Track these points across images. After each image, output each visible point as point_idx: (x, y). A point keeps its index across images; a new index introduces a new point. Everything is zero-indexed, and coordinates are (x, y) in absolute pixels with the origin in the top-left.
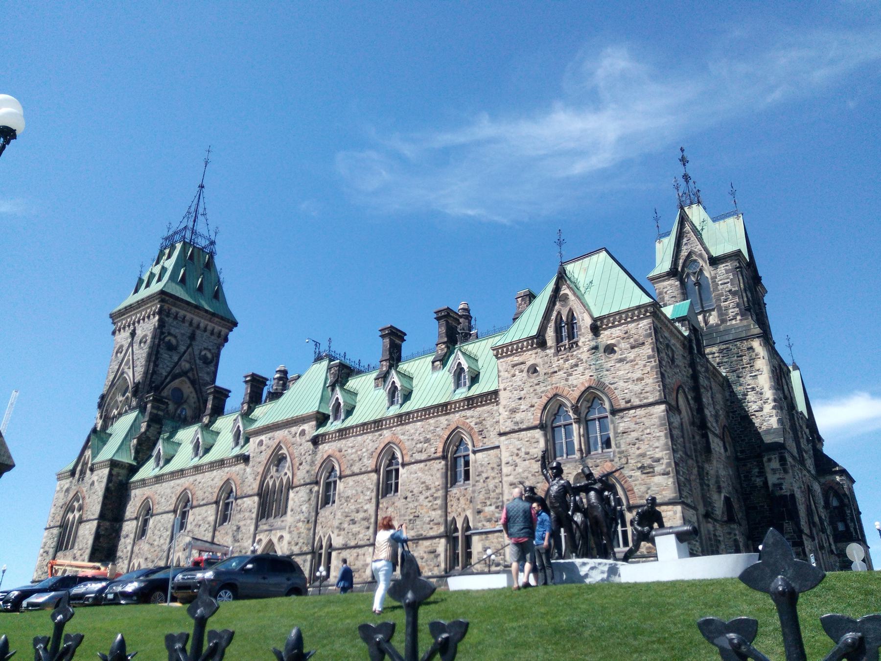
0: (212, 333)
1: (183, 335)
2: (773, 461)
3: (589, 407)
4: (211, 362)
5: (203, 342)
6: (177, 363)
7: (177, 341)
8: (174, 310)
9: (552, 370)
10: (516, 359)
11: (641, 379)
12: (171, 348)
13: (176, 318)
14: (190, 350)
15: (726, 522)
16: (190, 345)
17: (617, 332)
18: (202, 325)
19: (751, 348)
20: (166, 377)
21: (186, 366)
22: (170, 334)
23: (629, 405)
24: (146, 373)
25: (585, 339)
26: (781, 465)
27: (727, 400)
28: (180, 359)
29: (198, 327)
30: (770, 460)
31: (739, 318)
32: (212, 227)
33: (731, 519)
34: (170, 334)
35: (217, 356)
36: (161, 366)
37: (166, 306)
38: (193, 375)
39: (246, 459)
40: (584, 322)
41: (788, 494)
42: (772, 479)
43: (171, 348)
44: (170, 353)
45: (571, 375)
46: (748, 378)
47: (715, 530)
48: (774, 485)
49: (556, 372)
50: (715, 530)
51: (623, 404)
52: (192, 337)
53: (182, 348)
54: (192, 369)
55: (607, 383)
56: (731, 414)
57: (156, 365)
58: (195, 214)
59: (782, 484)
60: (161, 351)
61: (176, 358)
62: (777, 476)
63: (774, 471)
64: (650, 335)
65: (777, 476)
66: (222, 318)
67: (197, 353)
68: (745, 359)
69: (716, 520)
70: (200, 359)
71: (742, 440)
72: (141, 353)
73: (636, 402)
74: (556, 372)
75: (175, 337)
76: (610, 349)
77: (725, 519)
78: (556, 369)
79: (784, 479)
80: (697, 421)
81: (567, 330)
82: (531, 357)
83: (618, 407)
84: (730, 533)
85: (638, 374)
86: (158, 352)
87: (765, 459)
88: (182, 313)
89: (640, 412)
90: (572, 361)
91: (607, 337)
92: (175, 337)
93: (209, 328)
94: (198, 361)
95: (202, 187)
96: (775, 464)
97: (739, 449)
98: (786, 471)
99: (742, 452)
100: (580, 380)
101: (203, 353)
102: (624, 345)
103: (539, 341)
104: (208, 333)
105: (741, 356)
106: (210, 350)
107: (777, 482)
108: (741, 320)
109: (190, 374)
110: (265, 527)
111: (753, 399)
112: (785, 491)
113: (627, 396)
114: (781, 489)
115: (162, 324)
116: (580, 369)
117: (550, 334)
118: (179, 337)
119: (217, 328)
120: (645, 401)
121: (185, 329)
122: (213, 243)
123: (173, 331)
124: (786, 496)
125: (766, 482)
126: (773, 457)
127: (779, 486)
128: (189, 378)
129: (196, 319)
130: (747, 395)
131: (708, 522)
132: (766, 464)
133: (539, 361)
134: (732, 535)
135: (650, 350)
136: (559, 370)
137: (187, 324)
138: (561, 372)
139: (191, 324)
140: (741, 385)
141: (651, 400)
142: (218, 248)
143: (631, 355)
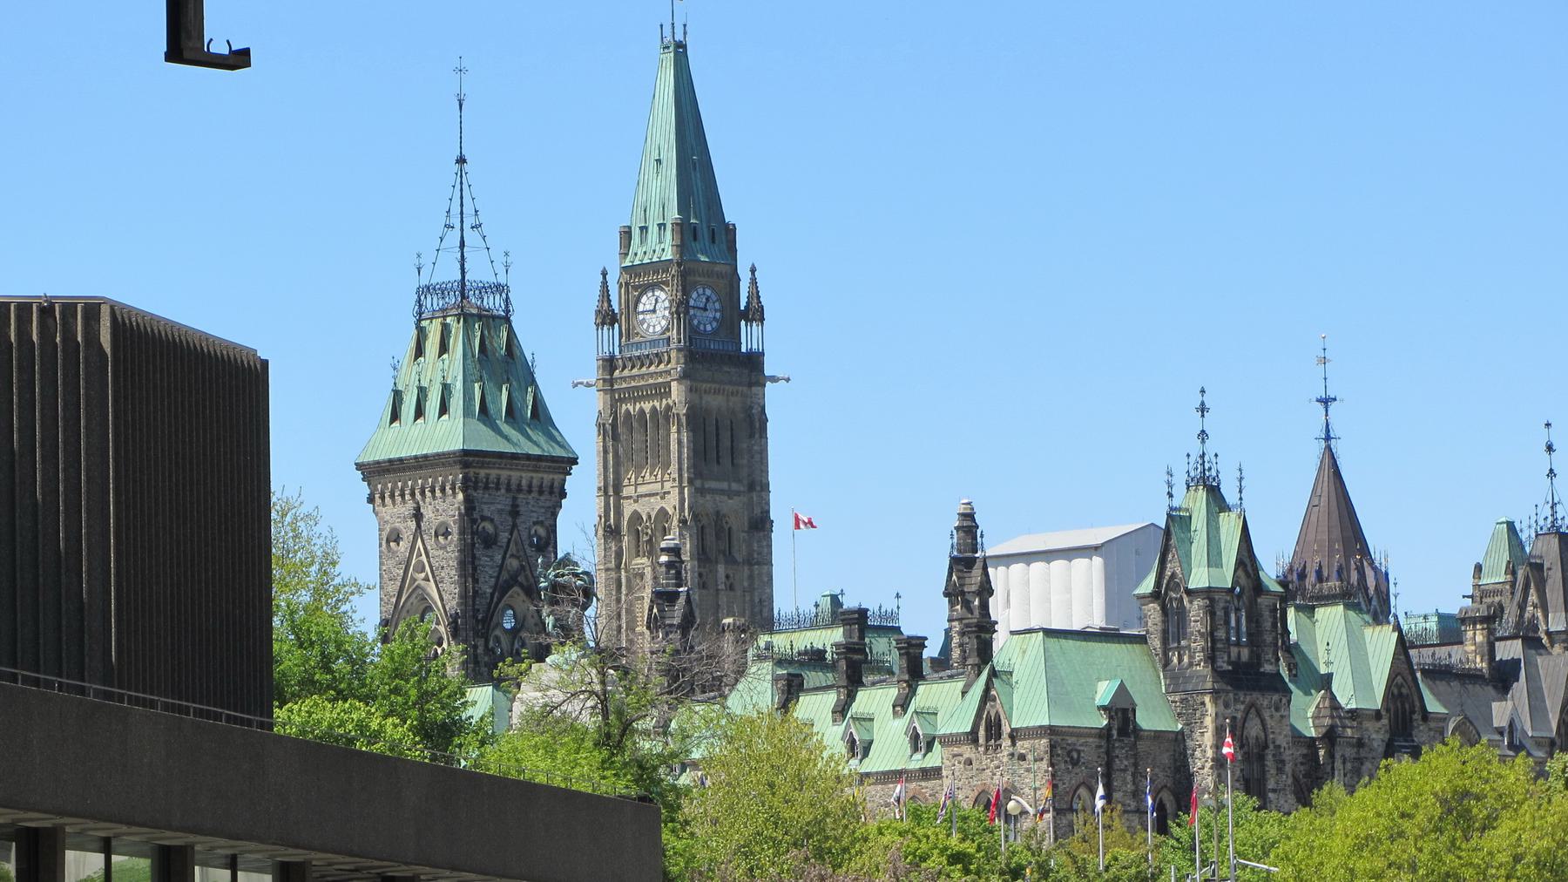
0: (541, 492)
1: (500, 512)
5: (531, 507)
7: (496, 528)
10: (956, 750)
12: (489, 542)
13: (486, 488)
16: (514, 526)
17: (1027, 744)
19: (1203, 703)
20: (492, 595)
22: (484, 518)
24: (464, 596)
25: (1006, 742)
28: (504, 558)
29: (519, 490)
34: (484, 518)
35: (552, 530)
36: (481, 580)
37: (471, 471)
40: (1006, 729)
43: (489, 542)
52: (515, 512)
53: (504, 536)
57: (476, 581)
60: (478, 553)
61: (498, 558)
67: (525, 535)
72: (446, 556)
75: (492, 520)
76: (1022, 757)
81: (994, 729)
82: (967, 751)
86: (474, 557)
88: (494, 473)
91: (1023, 746)
92: (492, 520)
93: (535, 482)
95: (461, 160)
103: (972, 738)
115: (468, 500)
117: (982, 732)
118: (496, 518)
119: (547, 477)
121: (502, 500)
123: (487, 513)
128: (521, 586)
133: (973, 756)
139: (508, 490)
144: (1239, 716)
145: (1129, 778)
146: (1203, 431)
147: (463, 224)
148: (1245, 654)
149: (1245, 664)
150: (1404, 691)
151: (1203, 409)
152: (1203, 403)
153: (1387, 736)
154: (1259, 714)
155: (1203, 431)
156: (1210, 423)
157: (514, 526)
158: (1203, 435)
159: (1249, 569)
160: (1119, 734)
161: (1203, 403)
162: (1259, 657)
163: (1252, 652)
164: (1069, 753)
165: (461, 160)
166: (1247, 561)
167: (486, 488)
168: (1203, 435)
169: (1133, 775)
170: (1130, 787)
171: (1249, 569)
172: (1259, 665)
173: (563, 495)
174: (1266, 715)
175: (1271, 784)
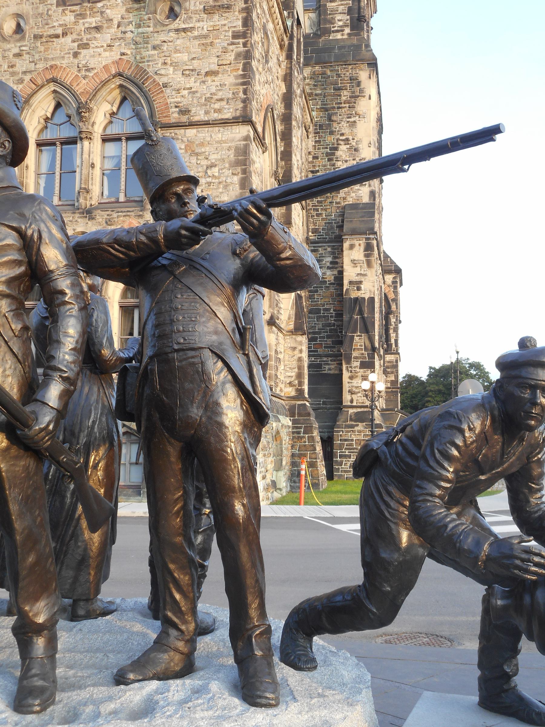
2: (357, 248)
3: (113, 114)
9: (52, 32)
15: (291, 331)
19: (355, 81)
23: (184, 119)
26: (366, 256)
27: (309, 153)
30: (352, 247)
31: (347, 30)
33: (298, 330)
41: (367, 297)
45: (86, 46)
47: (277, 344)
49: (57, 36)
50: (277, 344)
51: (174, 116)
55: (151, 71)
59: (361, 282)
62: (358, 270)
63: (354, 262)
65: (358, 270)
68: (345, 95)
69: (280, 329)
71: (318, 215)
73: (200, 115)
74: (57, 36)
77: (292, 327)
78: (59, 31)
79: (365, 275)
80: (281, 172)
83: (165, 120)
84: (294, 349)
87: (346, 245)
89: (204, 134)
90: (92, 21)
96: (358, 253)
97: (311, 227)
98: (369, 264)
99: (315, 231)
105: (340, 89)
107: (357, 279)
108: (349, 34)
111: (344, 157)
113: (184, 102)
114: (359, 289)
116: (105, 37)
120: (216, 116)
124: (364, 298)
125: (339, 278)
126: (357, 243)
127: (357, 285)
130: (336, 149)
131: (270, 332)
132: (345, 253)
134: (297, 352)
135: (240, 23)
136: (65, 34)
138: (69, 39)
140: (332, 133)
141: (228, 115)
143: (205, 25)
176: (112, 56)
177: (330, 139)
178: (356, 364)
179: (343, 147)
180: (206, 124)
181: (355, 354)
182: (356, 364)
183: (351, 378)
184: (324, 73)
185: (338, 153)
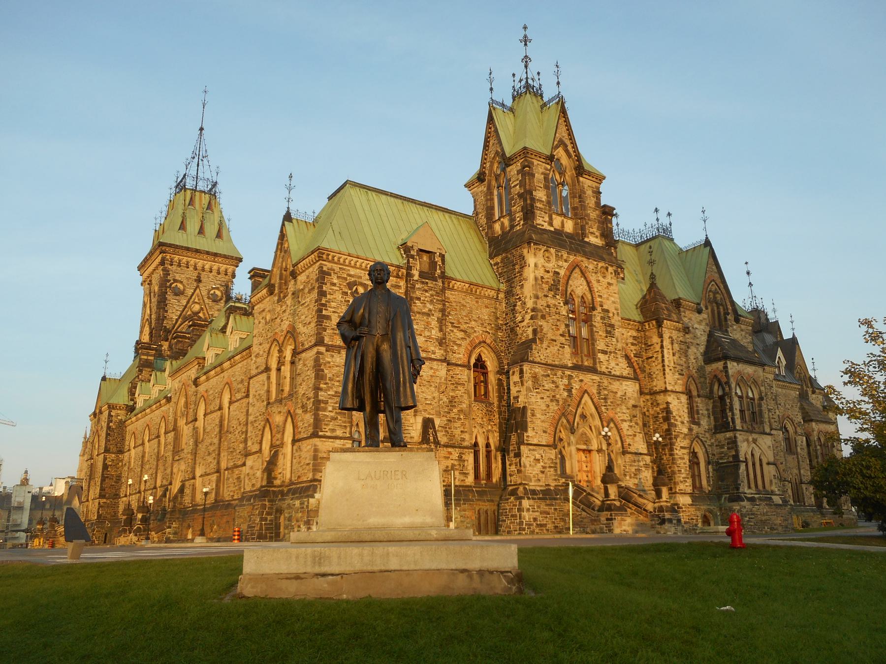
0: (219, 273)
4: (221, 299)
6: (186, 307)
8: (176, 258)
11: (310, 323)
13: (179, 265)
14: (198, 290)
16: (198, 287)
18: (207, 267)
20: (177, 320)
21: (196, 308)
28: (188, 302)
29: (203, 270)
30: (514, 373)
32: (213, 168)
34: (175, 281)
38: (204, 314)
39: (169, 400)
42: (514, 390)
44: (177, 297)
46: (518, 287)
48: (514, 398)
52: (199, 280)
53: (189, 292)
54: (202, 309)
56: (504, 327)
58: (199, 156)
61: (184, 302)
62: (517, 389)
63: (515, 383)
64: (317, 280)
66: (225, 257)
70: (209, 298)
85: (308, 320)
87: (511, 372)
92: (181, 282)
93: (215, 268)
94: (207, 301)
95: (201, 129)
98: (522, 385)
100: (285, 326)
101: (212, 292)
102: (306, 290)
104: (214, 273)
106: (217, 288)
107: (516, 394)
109: (201, 315)
110: (177, 458)
112: (521, 404)
118: (185, 281)
119: (223, 267)
121: (192, 274)
122: (215, 185)
127: (517, 398)
129: (200, 263)
130: (515, 306)
137: (191, 268)
139: (195, 269)
142: (219, 188)
144: (562, 272)
145: (434, 323)
146: (526, 57)
147: (199, 156)
148: (569, 227)
149: (569, 236)
150: (719, 297)
151: (526, 41)
152: (525, 36)
153: (708, 329)
154: (583, 274)
155: (526, 57)
156: (531, 50)
157: (198, 287)
158: (526, 60)
159: (570, 147)
160: (422, 275)
161: (525, 36)
162: (583, 228)
163: (576, 224)
164: (350, 285)
165: (201, 129)
166: (568, 142)
167: (179, 265)
168: (526, 60)
169: (441, 322)
170: (435, 333)
171: (570, 147)
172: (584, 235)
173: (234, 276)
174: (593, 278)
175: (600, 345)
176: (287, 323)
177: (512, 300)
178: (512, 455)
179: (519, 303)
180: (307, 349)
181: (511, 448)
182: (512, 455)
183: (510, 465)
184: (507, 257)
185: (517, 308)
